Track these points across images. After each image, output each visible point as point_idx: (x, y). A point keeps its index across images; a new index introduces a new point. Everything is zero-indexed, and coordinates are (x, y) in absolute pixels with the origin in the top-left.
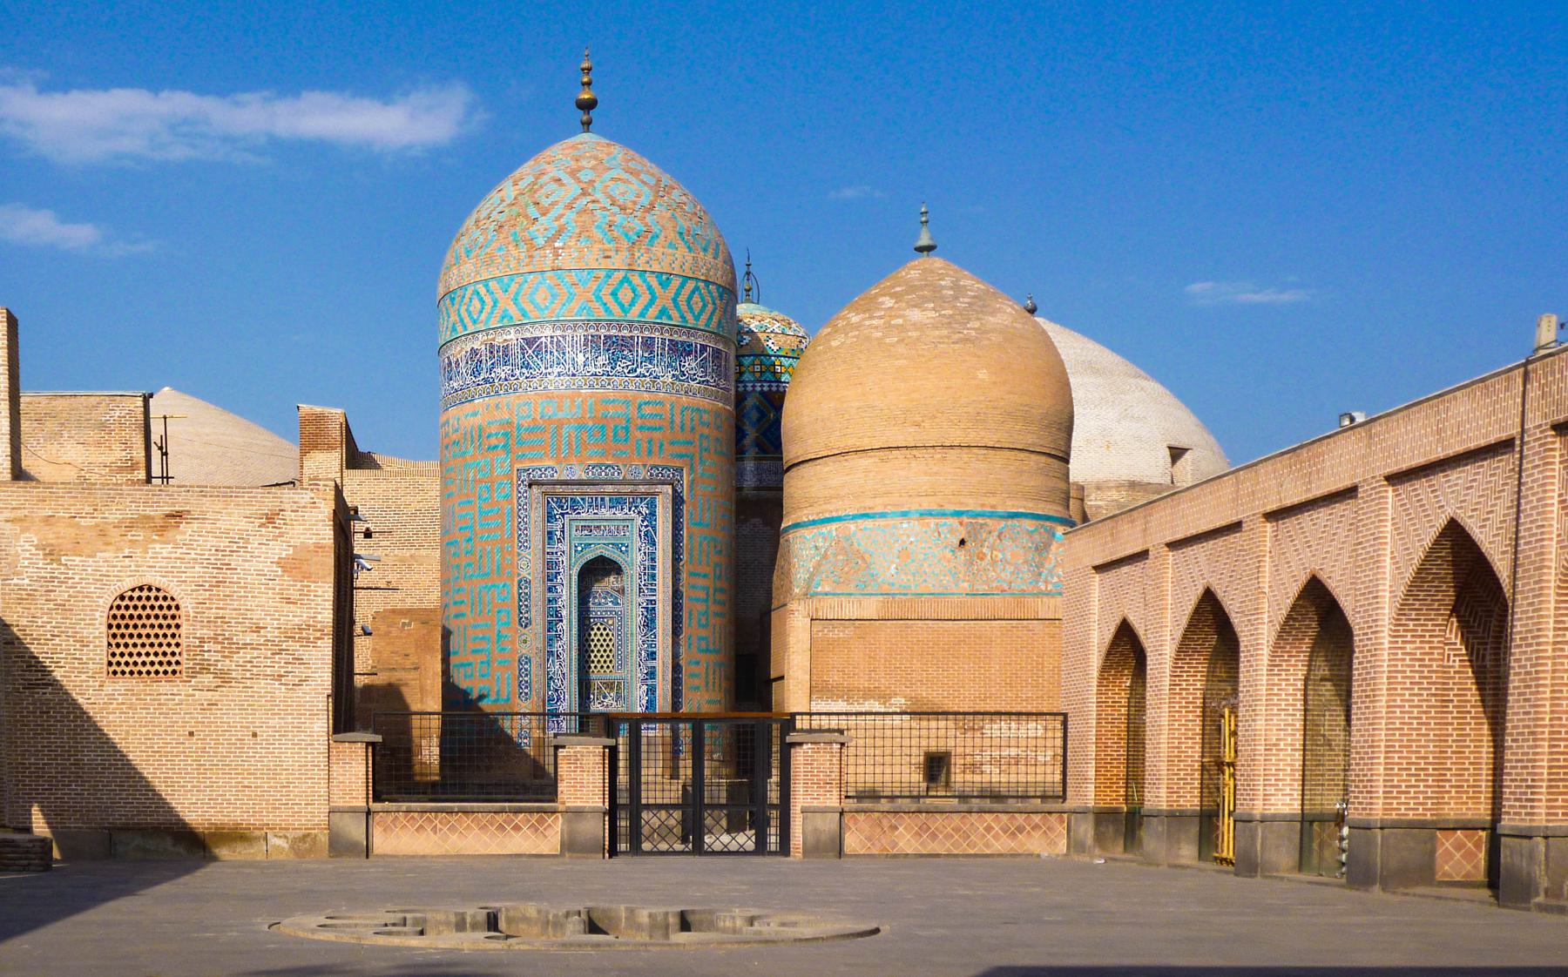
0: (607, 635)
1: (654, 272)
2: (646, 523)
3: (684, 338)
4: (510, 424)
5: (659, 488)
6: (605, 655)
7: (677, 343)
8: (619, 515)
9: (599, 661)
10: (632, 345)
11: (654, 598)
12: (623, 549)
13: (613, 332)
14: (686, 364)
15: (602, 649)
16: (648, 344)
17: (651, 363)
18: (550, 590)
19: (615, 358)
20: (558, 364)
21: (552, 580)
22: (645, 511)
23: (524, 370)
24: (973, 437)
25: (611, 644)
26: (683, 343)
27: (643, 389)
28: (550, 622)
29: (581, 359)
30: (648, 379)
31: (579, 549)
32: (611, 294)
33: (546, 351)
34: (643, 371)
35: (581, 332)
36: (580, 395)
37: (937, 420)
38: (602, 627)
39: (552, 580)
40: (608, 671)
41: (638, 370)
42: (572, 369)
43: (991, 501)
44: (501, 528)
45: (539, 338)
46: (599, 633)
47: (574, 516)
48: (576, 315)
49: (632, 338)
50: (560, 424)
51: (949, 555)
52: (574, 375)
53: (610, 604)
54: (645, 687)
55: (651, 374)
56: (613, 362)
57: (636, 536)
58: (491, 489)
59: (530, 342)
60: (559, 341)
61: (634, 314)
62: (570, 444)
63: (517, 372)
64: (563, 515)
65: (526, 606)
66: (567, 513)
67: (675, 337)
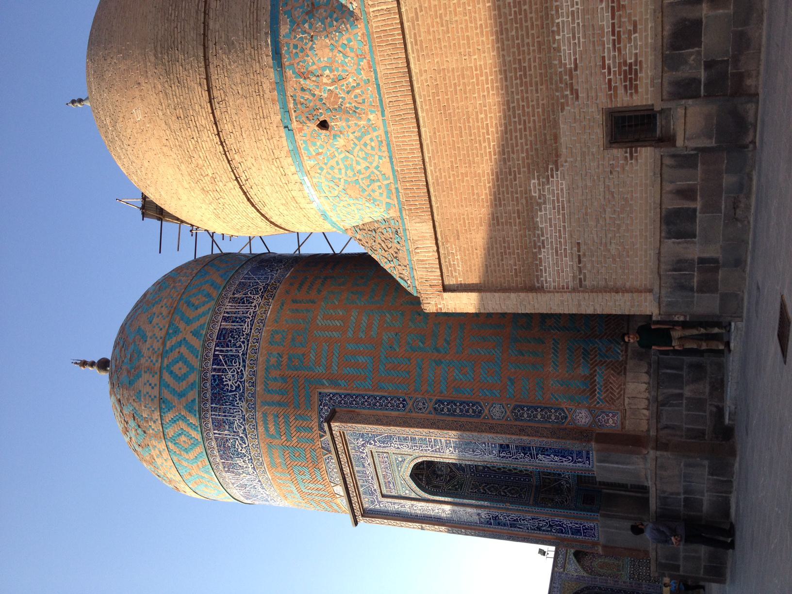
1: (161, 416)
2: (373, 442)
7: (213, 394)
8: (370, 460)
14: (230, 383)
24: (204, 120)
26: (213, 388)
30: (247, 427)
32: (187, 452)
34: (241, 431)
37: (201, 162)
43: (267, 86)
49: (216, 439)
51: (341, 142)
54: (540, 456)
61: (196, 435)
66: (377, 499)
67: (209, 395)
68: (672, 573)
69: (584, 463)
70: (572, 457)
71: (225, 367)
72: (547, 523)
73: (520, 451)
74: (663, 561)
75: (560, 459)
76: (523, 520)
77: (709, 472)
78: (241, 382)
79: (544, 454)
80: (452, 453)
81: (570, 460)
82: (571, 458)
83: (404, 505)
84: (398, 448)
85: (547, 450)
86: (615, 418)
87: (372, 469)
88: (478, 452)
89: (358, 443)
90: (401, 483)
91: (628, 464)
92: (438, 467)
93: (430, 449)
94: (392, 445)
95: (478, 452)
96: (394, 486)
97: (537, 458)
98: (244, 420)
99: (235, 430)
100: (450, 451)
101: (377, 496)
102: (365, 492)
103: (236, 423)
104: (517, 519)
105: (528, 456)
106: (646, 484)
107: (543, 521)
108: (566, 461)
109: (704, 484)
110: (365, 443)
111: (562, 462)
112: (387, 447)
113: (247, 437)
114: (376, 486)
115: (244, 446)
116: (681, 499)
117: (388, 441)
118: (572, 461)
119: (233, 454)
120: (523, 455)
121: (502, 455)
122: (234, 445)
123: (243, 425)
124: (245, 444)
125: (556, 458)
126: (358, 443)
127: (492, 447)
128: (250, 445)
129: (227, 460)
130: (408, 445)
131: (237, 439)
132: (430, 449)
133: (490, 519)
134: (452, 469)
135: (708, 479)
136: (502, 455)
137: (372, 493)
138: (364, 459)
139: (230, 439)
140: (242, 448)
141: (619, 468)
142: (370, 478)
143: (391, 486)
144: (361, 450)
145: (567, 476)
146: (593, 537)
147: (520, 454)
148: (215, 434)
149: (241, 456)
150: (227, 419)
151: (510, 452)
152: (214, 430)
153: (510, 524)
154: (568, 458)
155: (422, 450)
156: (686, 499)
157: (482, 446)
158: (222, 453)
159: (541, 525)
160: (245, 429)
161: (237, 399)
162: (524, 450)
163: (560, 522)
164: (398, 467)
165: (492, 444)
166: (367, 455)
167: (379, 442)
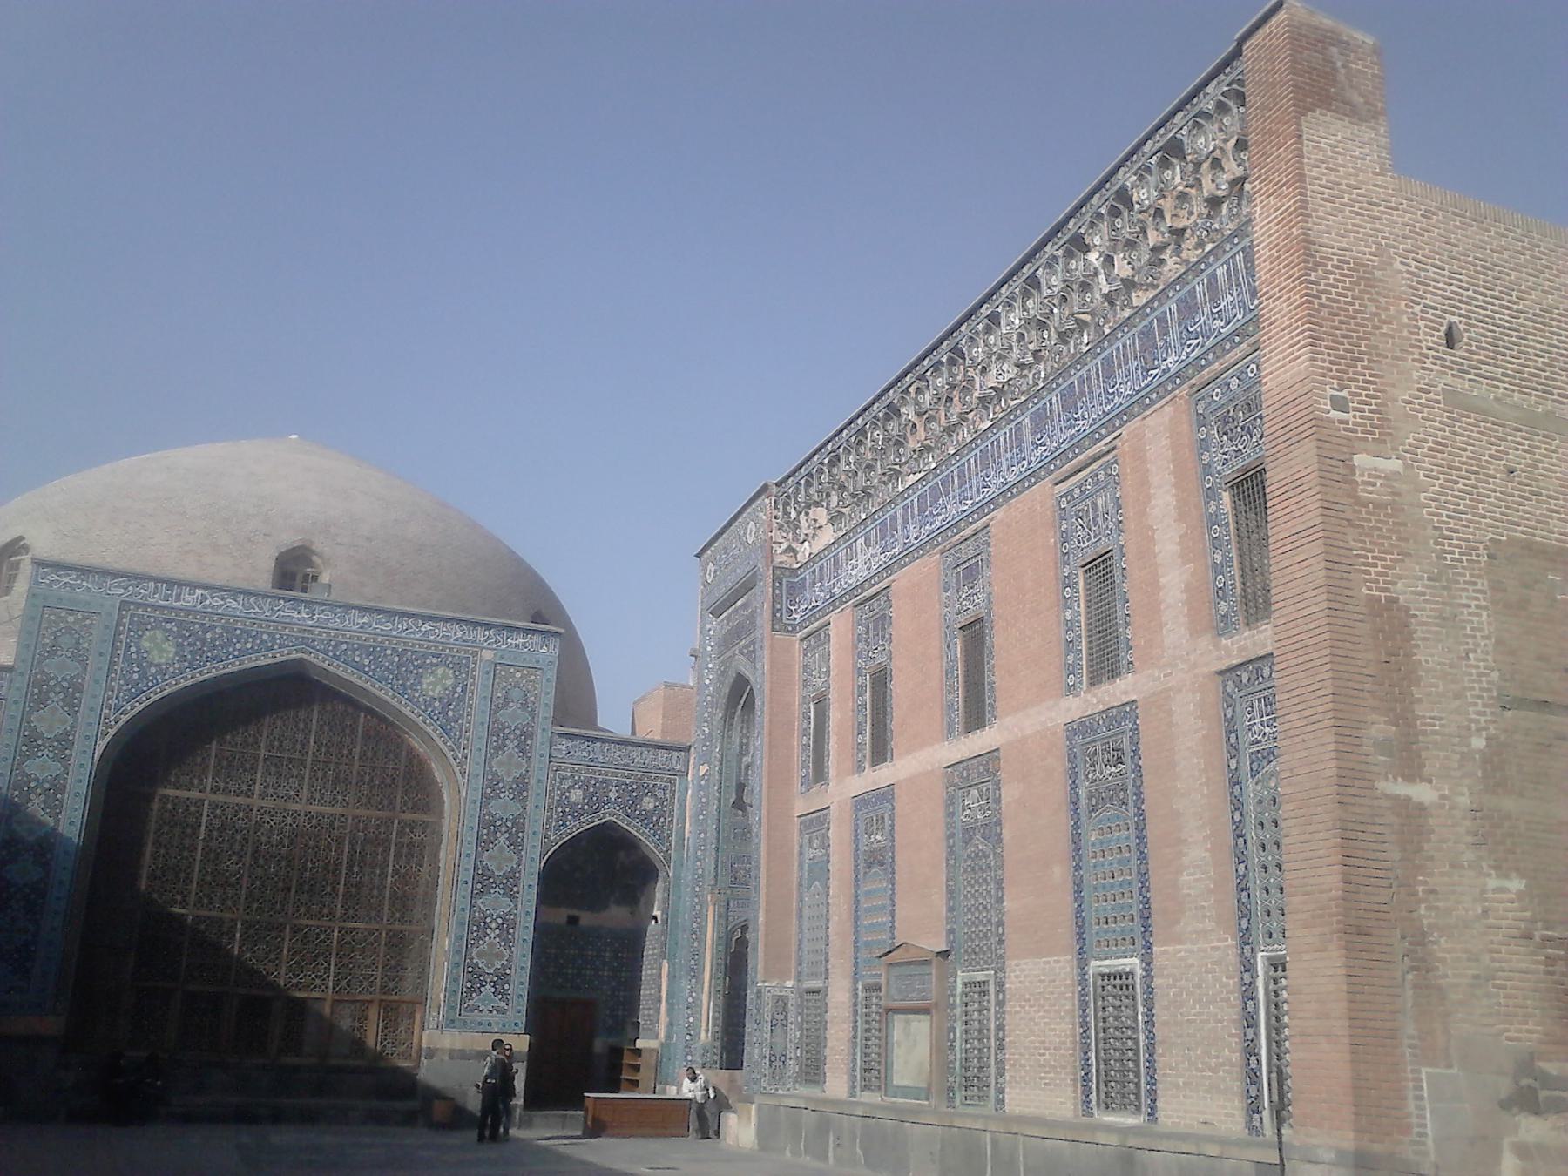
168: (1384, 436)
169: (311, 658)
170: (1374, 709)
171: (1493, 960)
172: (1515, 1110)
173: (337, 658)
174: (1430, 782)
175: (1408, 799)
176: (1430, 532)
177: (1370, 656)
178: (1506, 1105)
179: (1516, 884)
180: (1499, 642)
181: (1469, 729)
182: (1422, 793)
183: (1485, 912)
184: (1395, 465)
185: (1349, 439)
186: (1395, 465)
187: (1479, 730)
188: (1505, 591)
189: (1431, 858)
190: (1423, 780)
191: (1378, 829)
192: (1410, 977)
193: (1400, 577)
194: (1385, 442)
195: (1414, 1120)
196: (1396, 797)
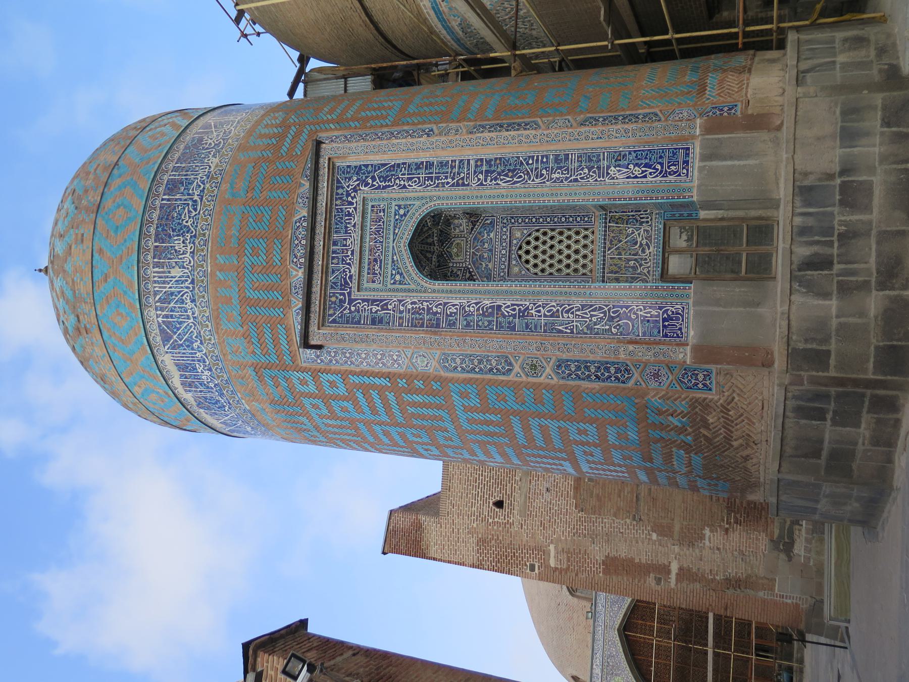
0: (537, 239)
2: (370, 181)
3: (182, 147)
4: (257, 368)
5: (324, 162)
6: (566, 242)
8: (357, 219)
9: (577, 252)
10: (169, 205)
11: (472, 162)
12: (402, 212)
13: (152, 230)
15: (558, 247)
16: (172, 187)
17: (191, 184)
18: (452, 325)
19: (179, 227)
20: (183, 302)
21: (438, 319)
22: (354, 183)
23: (195, 345)
25: (550, 234)
26: (186, 148)
27: (215, 192)
28: (500, 326)
29: (176, 272)
30: (208, 186)
31: (398, 277)
33: (172, 316)
35: (152, 272)
36: (213, 274)
38: (525, 247)
39: (438, 319)
40: (591, 237)
41: (196, 198)
42: (187, 284)
44: (381, 390)
45: (160, 326)
46: (533, 252)
47: (354, 285)
48: (132, 276)
49: (161, 207)
50: (245, 301)
52: (193, 282)
53: (492, 235)
55: (203, 183)
56: (182, 230)
57: (385, 194)
58: (336, 398)
59: (166, 338)
60: (160, 300)
62: (269, 288)
63: (199, 355)
64: (351, 301)
65: (480, 362)
66: (350, 294)
67: (176, 156)
68: (814, 373)
69: (679, 175)
70: (662, 167)
71: (213, 130)
72: (605, 313)
73: (583, 164)
74: (801, 346)
75: (643, 172)
76: (567, 312)
77: (883, 120)
78: (223, 140)
79: (619, 166)
80: (482, 184)
81: (658, 169)
82: (659, 167)
83: (386, 304)
84: (404, 187)
85: (625, 156)
86: (733, 111)
87: (356, 235)
88: (521, 177)
89: (348, 187)
90: (393, 259)
91: (748, 157)
92: (453, 271)
93: (449, 180)
94: (398, 181)
95: (521, 177)
96: (380, 267)
97: (608, 174)
98: (208, 178)
99: (191, 192)
100: (479, 179)
101: (350, 288)
102: (334, 283)
103: (195, 183)
104: (558, 310)
105: (594, 172)
106: (775, 196)
107: (600, 308)
108: (650, 174)
109: (874, 146)
110: (358, 185)
111: (645, 177)
112: (389, 186)
113: (201, 201)
114: (354, 270)
115: (194, 213)
116: (835, 186)
117: (392, 175)
118: (660, 173)
119: (174, 230)
120: (586, 171)
121: (557, 175)
122: (181, 215)
123: (204, 184)
124: (195, 210)
125: (637, 171)
126: (348, 187)
127: (542, 162)
128: (201, 212)
129: (163, 243)
130: (419, 178)
131: (188, 204)
132: (449, 180)
133: (514, 316)
134: (472, 276)
135: (882, 134)
136: (554, 176)
137: (346, 283)
138: (349, 214)
139: (178, 206)
140: (190, 217)
141: (733, 166)
142: (349, 253)
143: (377, 268)
144: (350, 199)
145: (645, 271)
146: (679, 337)
147: (582, 169)
148: (163, 200)
149: (182, 234)
150: (186, 179)
151: (567, 169)
152: (164, 195)
153: (546, 324)
154: (654, 168)
155: (437, 186)
156: (844, 186)
157: (528, 164)
158: (160, 229)
159: (594, 319)
160: (204, 188)
161: (211, 156)
162: (590, 160)
163: (627, 307)
164: (395, 227)
165: (543, 157)
166: (355, 208)
167: (379, 178)
168: (542, 551)
169: (617, 626)
170: (645, 582)
171: (736, 550)
172: (792, 554)
173: (616, 617)
174: (670, 562)
175: (677, 574)
176: (575, 538)
177: (625, 578)
178: (790, 559)
179: (707, 532)
180: (615, 515)
181: (649, 539)
182: (674, 568)
183: (718, 549)
184: (552, 547)
185: (545, 567)
186: (552, 547)
187: (649, 535)
188: (595, 506)
189: (699, 569)
190: (669, 566)
191: (688, 592)
192: (743, 589)
193: (594, 557)
194: (544, 550)
195: (794, 601)
196: (677, 580)
